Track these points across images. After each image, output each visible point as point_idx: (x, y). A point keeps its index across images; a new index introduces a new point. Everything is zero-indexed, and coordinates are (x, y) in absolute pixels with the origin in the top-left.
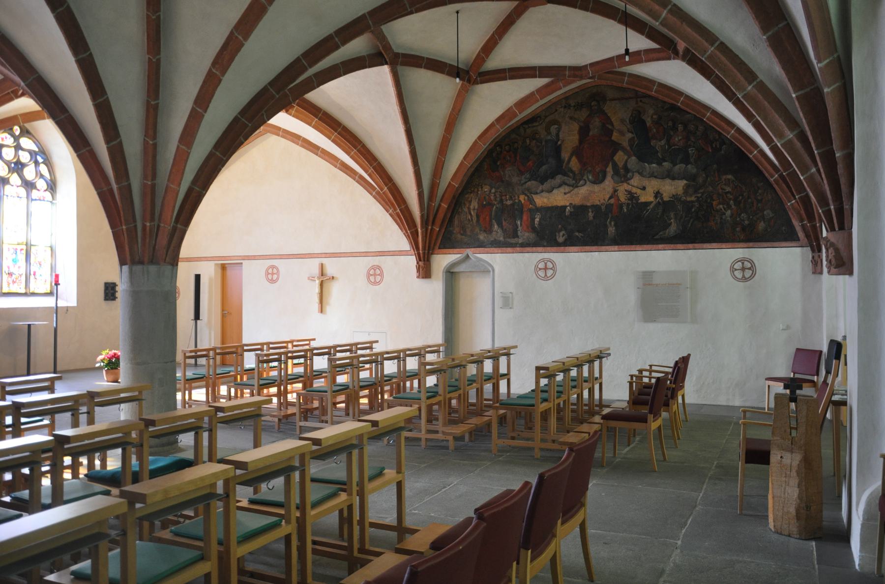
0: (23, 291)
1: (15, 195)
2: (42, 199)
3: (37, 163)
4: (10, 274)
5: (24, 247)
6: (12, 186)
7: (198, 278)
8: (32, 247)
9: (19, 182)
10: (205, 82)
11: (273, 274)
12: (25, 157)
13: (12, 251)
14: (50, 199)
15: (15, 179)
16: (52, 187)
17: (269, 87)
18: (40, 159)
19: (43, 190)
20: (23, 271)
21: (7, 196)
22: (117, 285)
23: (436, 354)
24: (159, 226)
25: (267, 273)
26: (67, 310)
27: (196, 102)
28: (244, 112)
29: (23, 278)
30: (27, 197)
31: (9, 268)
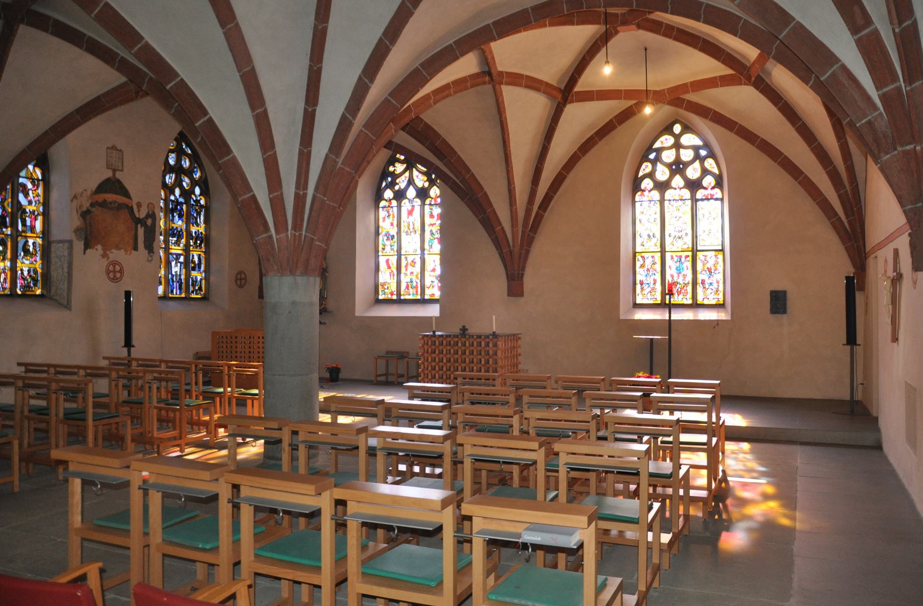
0: (690, 302)
2: (709, 197)
3: (702, 160)
5: (690, 254)
6: (675, 189)
8: (698, 253)
12: (687, 155)
13: (676, 259)
15: (678, 181)
18: (703, 153)
19: (710, 187)
20: (689, 278)
21: (670, 200)
29: (690, 288)
31: (672, 276)
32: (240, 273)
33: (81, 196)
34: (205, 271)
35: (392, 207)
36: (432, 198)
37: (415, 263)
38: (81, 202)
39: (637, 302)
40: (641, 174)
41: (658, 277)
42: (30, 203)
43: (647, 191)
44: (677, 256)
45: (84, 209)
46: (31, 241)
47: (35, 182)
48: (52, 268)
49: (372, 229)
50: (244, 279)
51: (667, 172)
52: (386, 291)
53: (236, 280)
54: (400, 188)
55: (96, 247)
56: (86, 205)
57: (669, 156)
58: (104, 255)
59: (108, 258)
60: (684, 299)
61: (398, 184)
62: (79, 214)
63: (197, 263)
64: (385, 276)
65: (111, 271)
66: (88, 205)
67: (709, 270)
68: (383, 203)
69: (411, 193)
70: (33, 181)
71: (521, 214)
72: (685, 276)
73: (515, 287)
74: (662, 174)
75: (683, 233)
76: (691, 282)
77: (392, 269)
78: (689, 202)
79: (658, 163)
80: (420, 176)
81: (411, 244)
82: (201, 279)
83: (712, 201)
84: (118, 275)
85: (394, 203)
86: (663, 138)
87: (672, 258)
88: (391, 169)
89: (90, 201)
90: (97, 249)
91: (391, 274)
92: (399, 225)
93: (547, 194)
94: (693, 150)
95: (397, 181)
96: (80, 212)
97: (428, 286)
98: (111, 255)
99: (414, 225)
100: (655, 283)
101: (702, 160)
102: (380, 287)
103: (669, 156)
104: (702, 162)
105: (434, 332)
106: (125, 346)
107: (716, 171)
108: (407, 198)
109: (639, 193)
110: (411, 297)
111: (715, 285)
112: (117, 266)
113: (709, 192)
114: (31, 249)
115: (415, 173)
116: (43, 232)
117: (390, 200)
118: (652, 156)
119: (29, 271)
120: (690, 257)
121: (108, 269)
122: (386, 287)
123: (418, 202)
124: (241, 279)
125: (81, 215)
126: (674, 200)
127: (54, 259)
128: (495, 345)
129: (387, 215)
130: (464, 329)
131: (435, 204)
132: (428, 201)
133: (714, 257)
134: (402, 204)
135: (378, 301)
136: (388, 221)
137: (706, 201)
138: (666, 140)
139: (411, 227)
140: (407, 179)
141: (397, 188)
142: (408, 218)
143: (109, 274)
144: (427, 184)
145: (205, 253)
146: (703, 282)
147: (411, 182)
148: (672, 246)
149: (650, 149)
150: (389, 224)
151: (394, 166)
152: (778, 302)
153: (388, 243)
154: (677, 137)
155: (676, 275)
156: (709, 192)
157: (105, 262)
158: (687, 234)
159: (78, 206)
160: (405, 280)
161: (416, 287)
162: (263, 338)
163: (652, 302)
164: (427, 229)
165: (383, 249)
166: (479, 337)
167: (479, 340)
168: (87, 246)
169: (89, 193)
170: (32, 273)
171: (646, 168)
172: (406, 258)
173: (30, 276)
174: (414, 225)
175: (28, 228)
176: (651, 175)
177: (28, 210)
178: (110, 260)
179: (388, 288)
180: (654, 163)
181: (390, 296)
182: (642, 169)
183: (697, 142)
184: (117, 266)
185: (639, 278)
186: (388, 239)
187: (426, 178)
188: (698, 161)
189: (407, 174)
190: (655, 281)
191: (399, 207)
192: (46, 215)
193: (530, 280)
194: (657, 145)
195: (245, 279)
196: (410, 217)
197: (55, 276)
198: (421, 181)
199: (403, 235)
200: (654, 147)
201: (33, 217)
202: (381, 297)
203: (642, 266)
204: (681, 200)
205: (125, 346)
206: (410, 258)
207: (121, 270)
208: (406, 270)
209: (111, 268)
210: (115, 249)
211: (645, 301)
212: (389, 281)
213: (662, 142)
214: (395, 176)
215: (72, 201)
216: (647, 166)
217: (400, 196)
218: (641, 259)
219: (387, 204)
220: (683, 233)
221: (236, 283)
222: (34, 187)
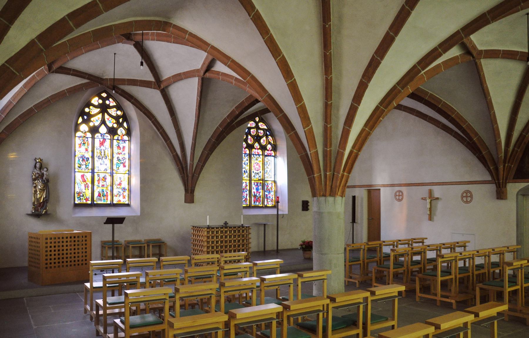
0: (261, 205)
3: (267, 136)
4: (255, 196)
6: (256, 149)
7: (354, 198)
9: (258, 147)
10: (358, 88)
11: (399, 196)
12: (261, 133)
13: (256, 184)
14: (273, 155)
15: (257, 145)
16: (275, 148)
17: (397, 86)
18: (268, 133)
20: (261, 194)
21: (253, 154)
22: (309, 202)
23: (513, 253)
24: (334, 174)
25: (396, 195)
26: (283, 216)
27: (354, 100)
28: (382, 102)
29: (261, 199)
31: (254, 192)
35: (87, 138)
36: (119, 136)
52: (82, 197)
64: (79, 187)
68: (78, 134)
69: (103, 129)
72: (259, 193)
73: (190, 197)
75: (259, 171)
76: (262, 197)
80: (110, 119)
81: (102, 166)
87: (254, 184)
88: (87, 110)
91: (86, 186)
92: (93, 152)
95: (92, 119)
99: (104, 152)
100: (246, 196)
102: (76, 195)
103: (253, 132)
104: (267, 137)
107: (272, 142)
108: (99, 132)
110: (102, 202)
111: (271, 197)
113: (269, 152)
115: (106, 116)
117: (85, 132)
123: (108, 136)
126: (255, 154)
129: (83, 143)
130: (226, 223)
131: (121, 140)
132: (116, 137)
133: (271, 184)
134: (95, 137)
138: (251, 124)
139: (103, 154)
140: (100, 119)
141: (91, 124)
142: (100, 147)
144: (115, 126)
146: (267, 195)
147: (103, 122)
150: (85, 150)
151: (89, 108)
152: (305, 206)
154: (257, 123)
155: (256, 192)
158: (260, 172)
161: (107, 196)
164: (116, 156)
166: (235, 227)
172: (98, 175)
174: (104, 152)
176: (246, 140)
181: (85, 201)
183: (265, 127)
186: (83, 160)
187: (114, 121)
190: (247, 195)
191: (93, 138)
193: (198, 194)
194: (249, 125)
196: (102, 146)
199: (96, 159)
202: (76, 202)
204: (258, 155)
206: (102, 175)
208: (99, 183)
212: (84, 190)
213: (251, 124)
214: (89, 116)
217: (94, 130)
219: (83, 135)
220: (259, 171)
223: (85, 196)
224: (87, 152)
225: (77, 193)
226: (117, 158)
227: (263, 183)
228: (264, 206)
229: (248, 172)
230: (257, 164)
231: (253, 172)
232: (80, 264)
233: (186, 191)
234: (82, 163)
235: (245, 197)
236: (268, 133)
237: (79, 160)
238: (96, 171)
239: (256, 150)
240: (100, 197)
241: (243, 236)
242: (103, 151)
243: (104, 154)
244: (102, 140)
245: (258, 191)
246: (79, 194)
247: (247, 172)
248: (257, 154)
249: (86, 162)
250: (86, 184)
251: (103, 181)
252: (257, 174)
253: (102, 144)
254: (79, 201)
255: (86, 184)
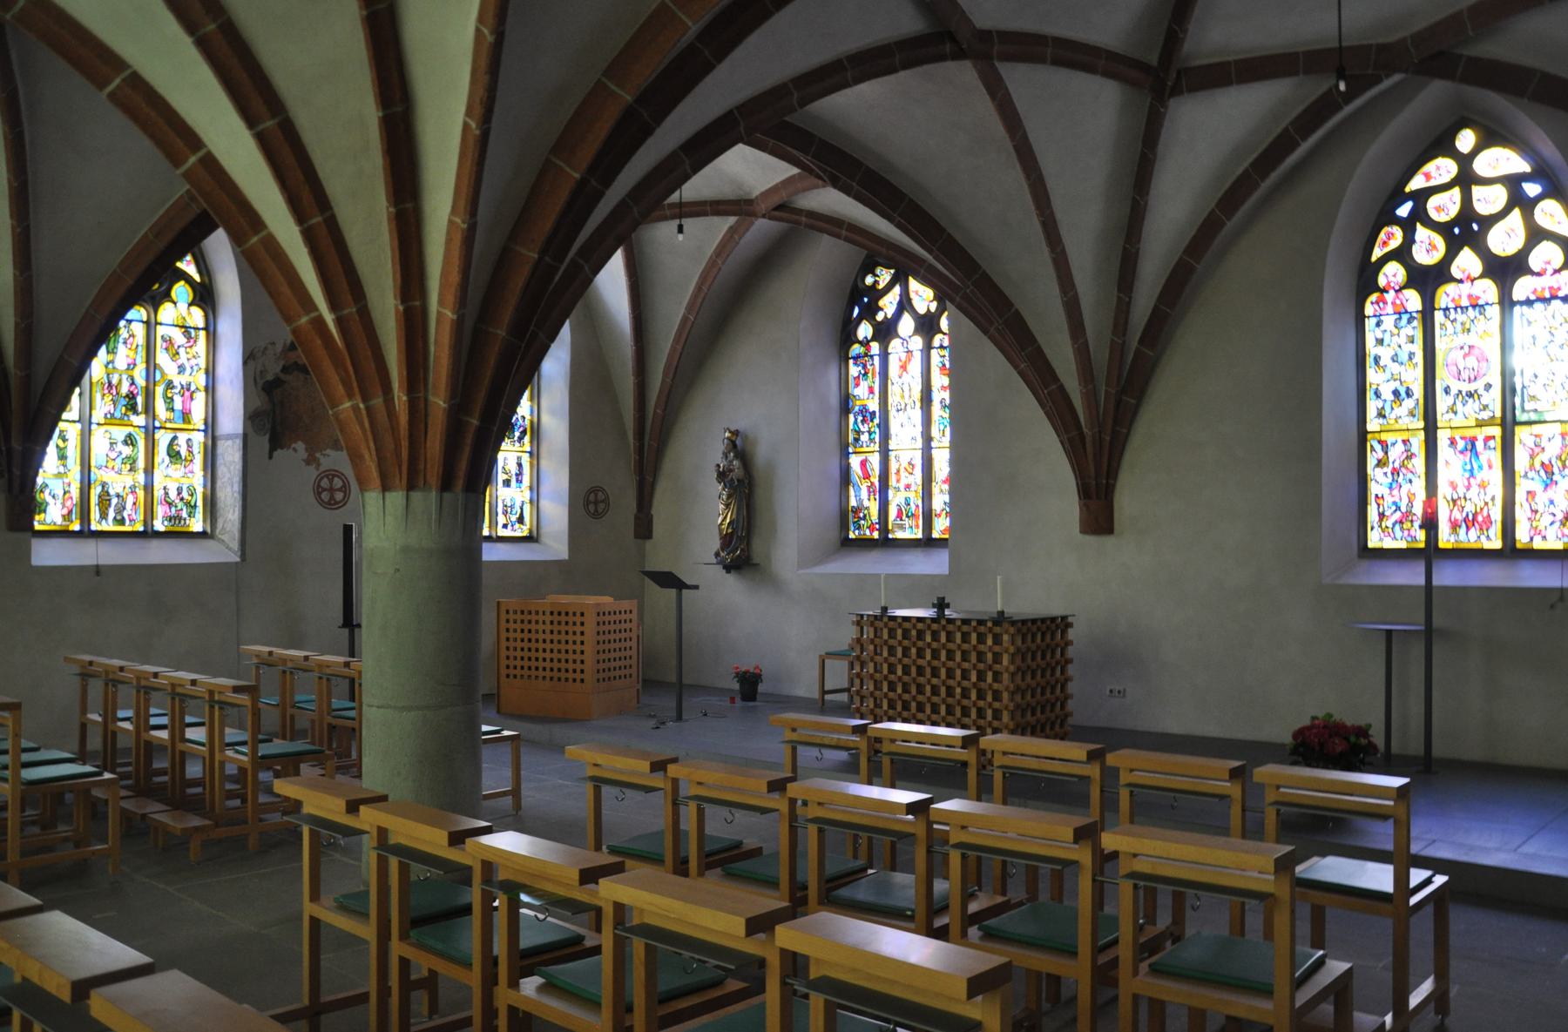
0: (1496, 544)
1: (1465, 302)
2: (1547, 295)
5: (1496, 431)
6: (1461, 281)
8: (1518, 429)
12: (1489, 200)
13: (1461, 444)
15: (1467, 262)
19: (1550, 271)
21: (1447, 309)
30: (1501, 302)
32: (595, 490)
33: (263, 353)
34: (531, 488)
35: (872, 356)
36: (945, 334)
37: (913, 466)
38: (264, 366)
39: (1371, 545)
40: (1377, 253)
41: (1419, 487)
42: (181, 369)
43: (1392, 293)
44: (1462, 438)
45: (270, 377)
46: (182, 438)
47: (190, 333)
48: (219, 484)
49: (834, 400)
50: (603, 501)
51: (1440, 242)
52: (862, 522)
53: (587, 503)
54: (886, 317)
55: (293, 445)
56: (274, 369)
57: (1445, 207)
58: (311, 460)
59: (319, 465)
60: (1483, 538)
61: (882, 309)
62: (260, 388)
63: (513, 473)
65: (324, 490)
66: (278, 369)
67: (1547, 468)
68: (856, 349)
69: (906, 325)
70: (186, 329)
71: (1100, 355)
72: (1483, 486)
74: (1428, 248)
75: (1479, 385)
77: (872, 479)
78: (1494, 312)
79: (1418, 225)
82: (523, 503)
83: (1556, 303)
84: (339, 496)
85: (875, 347)
86: (1430, 167)
87: (1453, 442)
89: (282, 363)
90: (295, 450)
93: (1155, 310)
94: (1503, 184)
95: (881, 303)
96: (261, 383)
97: (938, 512)
98: (322, 460)
101: (1527, 205)
102: (851, 514)
105: (885, 609)
106: (344, 626)
109: (1374, 297)
112: (336, 479)
114: (184, 452)
116: (206, 423)
117: (868, 342)
118: (1404, 211)
119: (179, 491)
120: (1499, 440)
121: (319, 486)
122: (861, 515)
123: (917, 343)
124: (596, 503)
125: (263, 389)
127: (222, 471)
128: (997, 640)
129: (863, 372)
132: (937, 340)
135: (846, 543)
136: (864, 385)
137: (1538, 306)
138: (1442, 169)
140: (898, 298)
141: (880, 317)
143: (319, 494)
145: (531, 453)
147: (905, 304)
148: (1451, 415)
149: (1399, 197)
153: (864, 428)
154: (1465, 161)
156: (1547, 281)
157: (312, 473)
158: (1488, 387)
159: (258, 373)
160: (896, 499)
162: (582, 614)
163: (1403, 545)
165: (857, 440)
167: (965, 628)
168: (276, 443)
169: (279, 348)
170: (185, 494)
171: (1393, 237)
173: (182, 499)
175: (178, 414)
176: (1402, 254)
177: (176, 383)
178: (322, 469)
179: (865, 516)
180: (1408, 226)
181: (868, 532)
182: (1379, 240)
184: (336, 479)
185: (1374, 489)
188: (1516, 213)
189: (897, 290)
191: (885, 356)
192: (211, 389)
193: (1127, 500)
194: (1417, 183)
195: (606, 501)
197: (223, 498)
198: (923, 297)
199: (892, 413)
200: (1407, 190)
201: (187, 394)
202: (852, 536)
203: (1380, 463)
204: (1474, 306)
205: (344, 626)
207: (344, 486)
208: (898, 481)
209: (325, 483)
210: (332, 448)
211: (1389, 544)
215: (245, 363)
216: (1390, 236)
217: (885, 332)
218: (1378, 447)
219: (862, 350)
221: (588, 512)
222: (188, 342)
223: (868, 517)
224: (871, 396)
225: (852, 511)
226: (941, 402)
227: (1504, 438)
228: (494, 535)
229: (1418, 391)
230: (1466, 349)
231: (1447, 391)
232: (563, 679)
233: (1085, 492)
234: (862, 429)
235: (1404, 510)
236: (1532, 189)
237: (856, 419)
238: (892, 445)
239: (1467, 284)
240: (901, 520)
241: (981, 656)
242: (906, 388)
243: (910, 397)
244: (904, 357)
245: (1472, 475)
246: (856, 510)
247: (1409, 393)
248: (1465, 302)
249: (871, 424)
250: (869, 484)
251: (907, 474)
252: (1470, 395)
253: (904, 367)
254: (857, 532)
255: (869, 484)
